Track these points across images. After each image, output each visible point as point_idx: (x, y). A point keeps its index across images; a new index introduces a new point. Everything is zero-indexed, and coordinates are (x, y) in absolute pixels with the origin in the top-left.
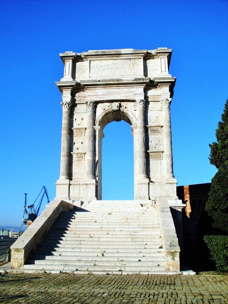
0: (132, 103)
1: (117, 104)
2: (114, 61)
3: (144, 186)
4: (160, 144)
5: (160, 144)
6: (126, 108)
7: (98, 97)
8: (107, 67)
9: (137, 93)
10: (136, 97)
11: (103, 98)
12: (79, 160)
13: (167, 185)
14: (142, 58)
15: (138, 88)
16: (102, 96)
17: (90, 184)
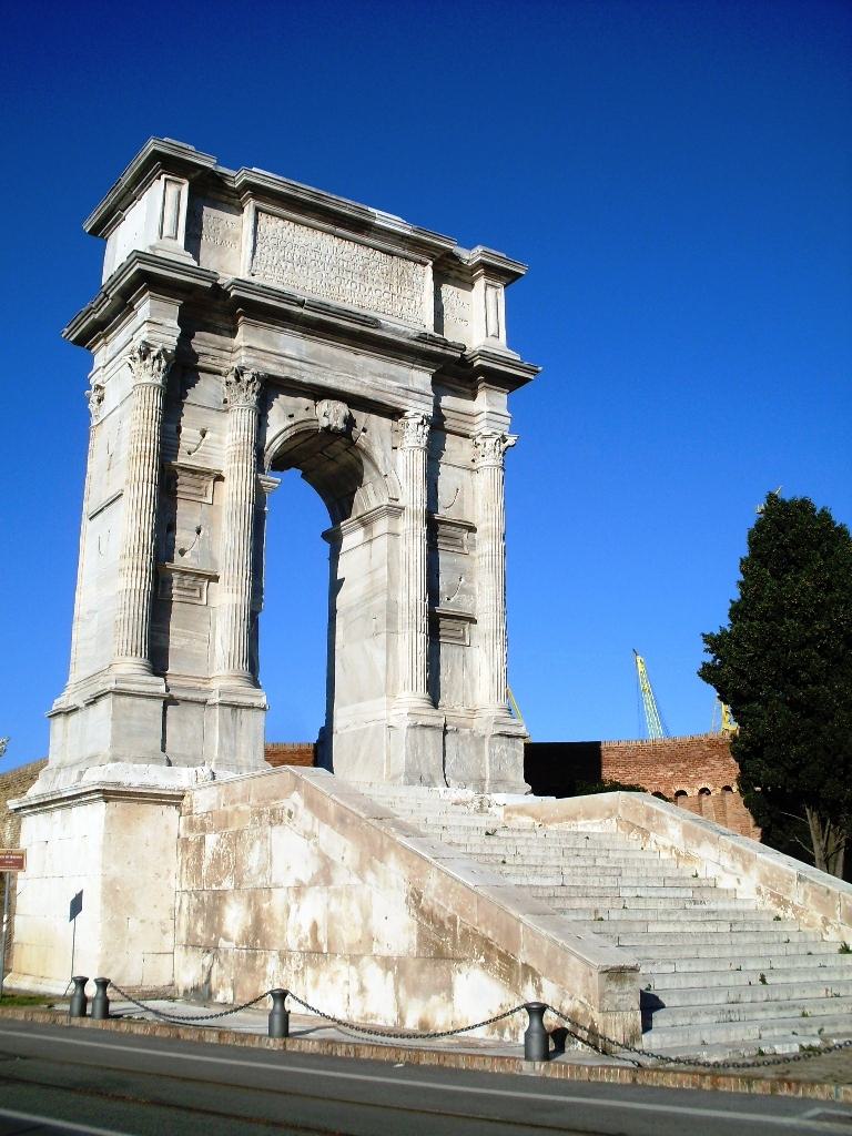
0: (386, 422)
1: (342, 409)
2: (336, 241)
3: (428, 733)
4: (464, 591)
5: (464, 591)
6: (364, 430)
7: (281, 364)
8: (313, 256)
9: (411, 386)
10: (410, 402)
11: (299, 372)
12: (185, 600)
13: (498, 738)
14: (431, 263)
15: (416, 369)
16: (297, 363)
17: (251, 707)
